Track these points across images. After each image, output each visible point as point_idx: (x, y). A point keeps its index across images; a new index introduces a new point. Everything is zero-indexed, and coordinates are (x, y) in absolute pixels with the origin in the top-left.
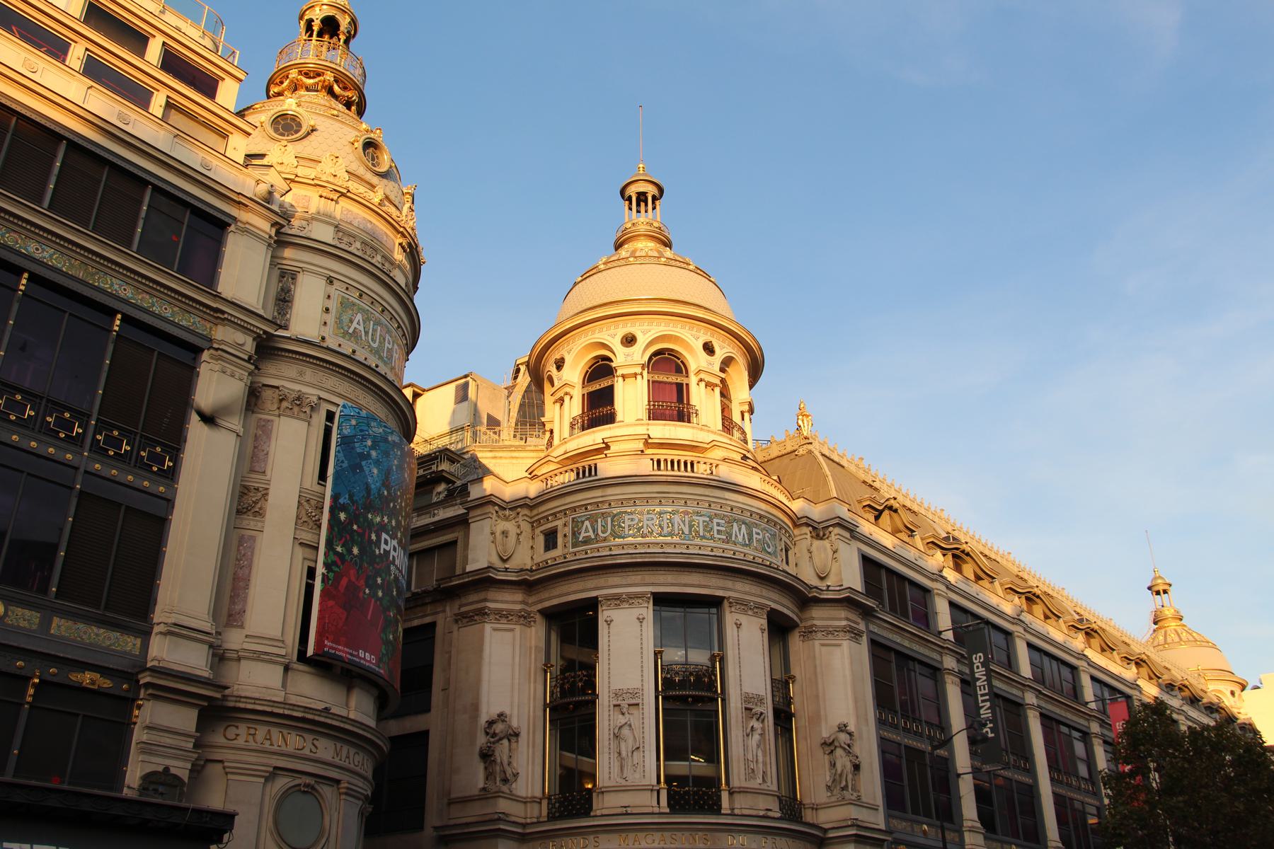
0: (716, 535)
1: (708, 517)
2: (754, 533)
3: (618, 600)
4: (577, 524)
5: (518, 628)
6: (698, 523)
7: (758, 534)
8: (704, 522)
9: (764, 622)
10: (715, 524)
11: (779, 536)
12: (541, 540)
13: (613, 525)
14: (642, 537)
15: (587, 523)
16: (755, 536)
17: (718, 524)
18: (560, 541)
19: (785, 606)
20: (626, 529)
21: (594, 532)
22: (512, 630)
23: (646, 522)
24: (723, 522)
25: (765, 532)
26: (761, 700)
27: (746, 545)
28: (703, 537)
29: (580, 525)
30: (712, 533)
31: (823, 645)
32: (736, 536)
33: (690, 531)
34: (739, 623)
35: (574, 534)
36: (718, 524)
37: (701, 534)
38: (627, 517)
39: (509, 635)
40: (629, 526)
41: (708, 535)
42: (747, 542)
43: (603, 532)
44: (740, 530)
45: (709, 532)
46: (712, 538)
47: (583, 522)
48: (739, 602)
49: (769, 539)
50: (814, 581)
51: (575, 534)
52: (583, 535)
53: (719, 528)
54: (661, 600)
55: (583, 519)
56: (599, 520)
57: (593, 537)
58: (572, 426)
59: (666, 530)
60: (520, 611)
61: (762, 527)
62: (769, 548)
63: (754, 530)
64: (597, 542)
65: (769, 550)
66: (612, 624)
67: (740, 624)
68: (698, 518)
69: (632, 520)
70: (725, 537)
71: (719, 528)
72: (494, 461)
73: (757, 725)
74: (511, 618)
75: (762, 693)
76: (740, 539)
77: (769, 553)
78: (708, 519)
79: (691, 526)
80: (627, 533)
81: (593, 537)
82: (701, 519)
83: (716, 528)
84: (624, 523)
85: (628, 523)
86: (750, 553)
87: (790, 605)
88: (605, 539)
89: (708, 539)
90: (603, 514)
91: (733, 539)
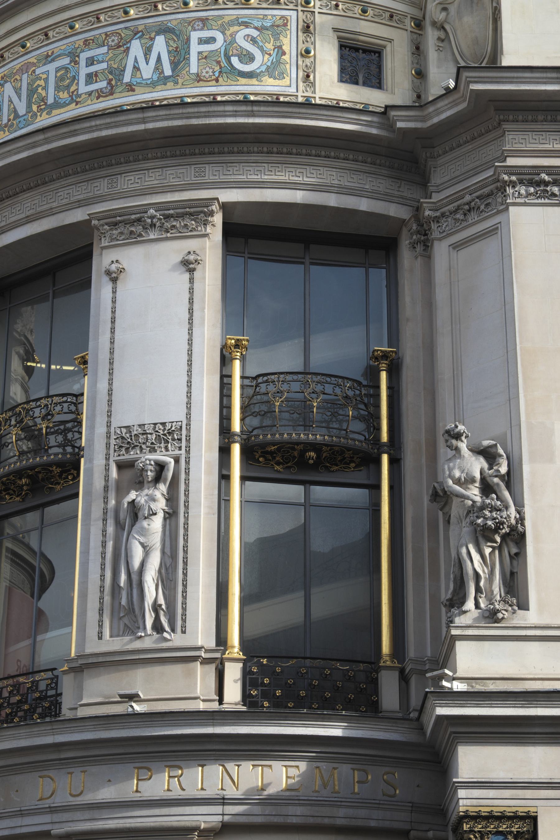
6: (46, 80)
16: (195, 48)
24: (105, 49)
27: (164, 80)
30: (73, 89)
32: (136, 68)
36: (91, 62)
42: (168, 72)
44: (147, 52)
67: (121, 271)
70: (103, 84)
76: (147, 71)
91: (127, 78)
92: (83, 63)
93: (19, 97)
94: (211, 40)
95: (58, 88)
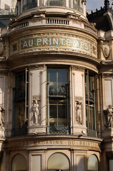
0: (67, 45)
1: (65, 38)
2: (81, 43)
3: (34, 67)
4: (22, 42)
5: (4, 76)
6: (61, 41)
7: (82, 44)
8: (63, 40)
9: (83, 73)
10: (67, 41)
11: (90, 44)
12: (12, 49)
13: (33, 42)
14: (43, 46)
15: (25, 42)
16: (81, 44)
17: (68, 41)
18: (17, 47)
19: (94, 68)
20: (38, 44)
21: (27, 44)
22: (3, 77)
23: (44, 41)
25: (85, 43)
26: (81, 99)
27: (78, 48)
28: (63, 45)
29: (23, 42)
30: (66, 44)
31: (105, 80)
32: (74, 44)
33: (59, 43)
34: (74, 73)
35: (21, 45)
36: (68, 41)
37: (62, 44)
38: (38, 40)
39: (2, 78)
40: (39, 42)
41: (64, 45)
42: (78, 47)
43: (30, 45)
45: (65, 43)
46: (66, 45)
47: (24, 41)
48: (74, 66)
49: (87, 45)
50: (103, 58)
51: (22, 45)
52: (24, 46)
53: (68, 42)
54: (49, 67)
55: (24, 40)
56: (29, 41)
57: (27, 46)
58: (23, 8)
59: (50, 43)
60: (5, 71)
61: (84, 41)
62: (86, 48)
63: (81, 42)
64: (28, 48)
65: (86, 49)
66: (33, 75)
68: (62, 39)
69: (39, 40)
70: (70, 45)
71: (68, 42)
72: (4, 21)
73: (80, 106)
74: (2, 73)
75: (82, 96)
76: (76, 45)
77: (86, 50)
78: (65, 39)
79: (59, 42)
80: (38, 45)
81: (27, 46)
82: (62, 39)
83: (67, 42)
84: (37, 41)
85: (38, 41)
86: (80, 49)
87: (95, 68)
88: (31, 47)
89: (64, 46)
90: (30, 38)
92: (67, 41)
93: (57, 41)
94: (82, 44)
95: (63, 43)
